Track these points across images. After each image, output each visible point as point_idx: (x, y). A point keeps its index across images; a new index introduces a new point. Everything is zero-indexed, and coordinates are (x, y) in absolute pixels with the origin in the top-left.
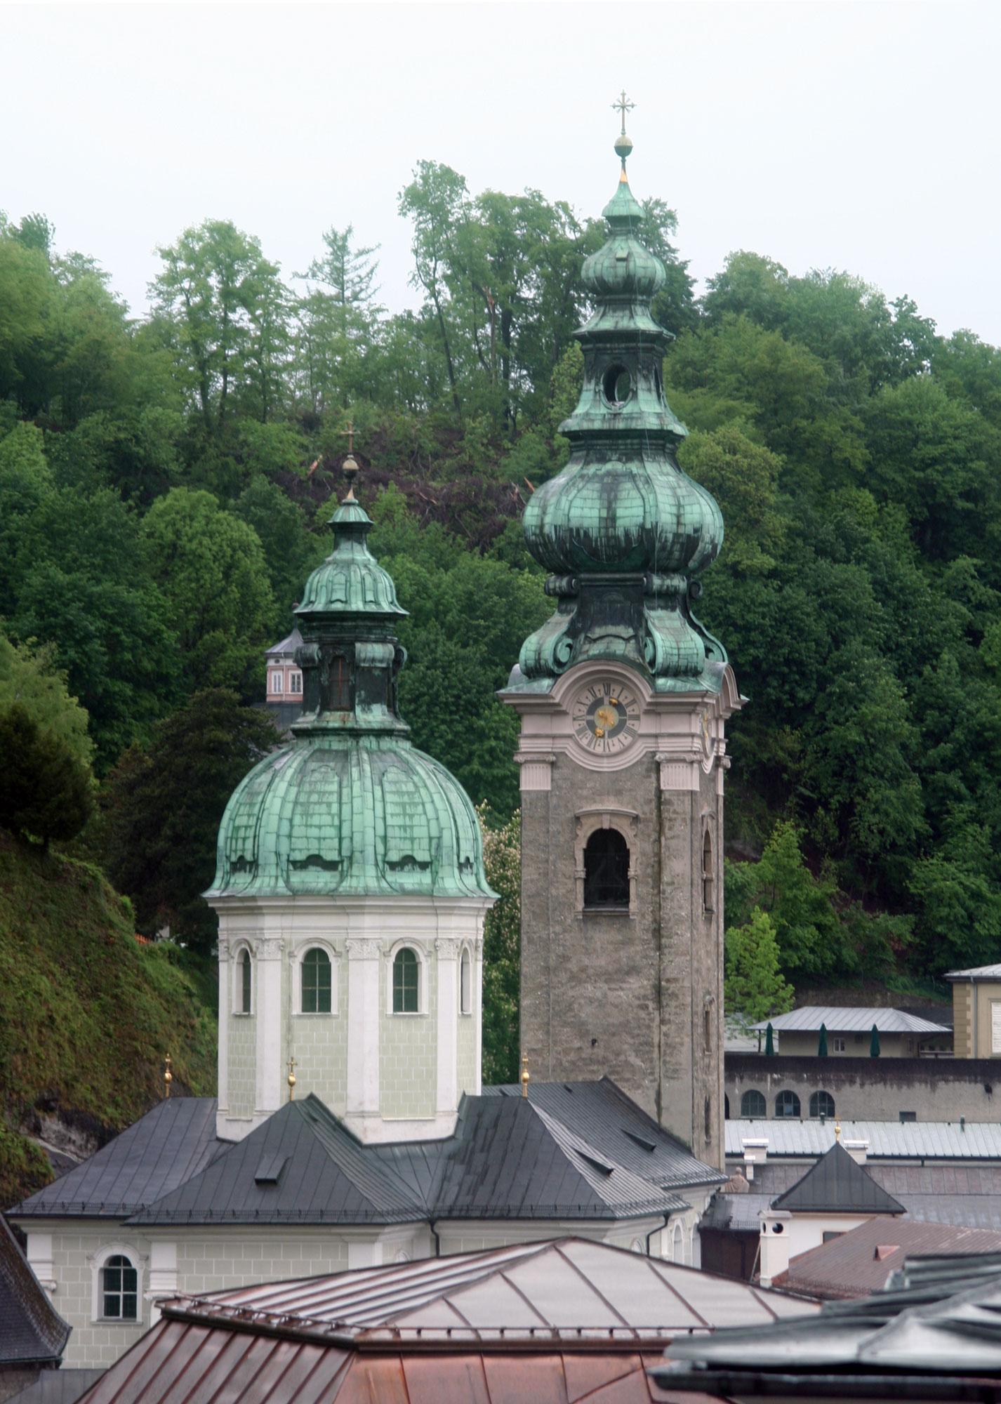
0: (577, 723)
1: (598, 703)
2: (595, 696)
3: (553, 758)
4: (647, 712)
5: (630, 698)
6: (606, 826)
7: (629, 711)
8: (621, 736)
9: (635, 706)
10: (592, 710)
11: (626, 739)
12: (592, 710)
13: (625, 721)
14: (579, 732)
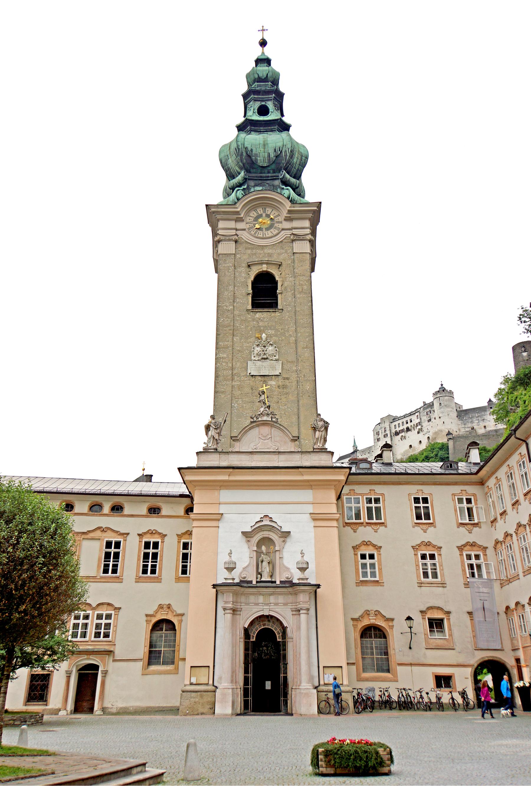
0: (248, 225)
1: (260, 216)
3: (236, 237)
4: (285, 220)
5: (277, 214)
6: (265, 269)
8: (272, 230)
9: (279, 217)
11: (274, 231)
13: (274, 224)
14: (249, 229)
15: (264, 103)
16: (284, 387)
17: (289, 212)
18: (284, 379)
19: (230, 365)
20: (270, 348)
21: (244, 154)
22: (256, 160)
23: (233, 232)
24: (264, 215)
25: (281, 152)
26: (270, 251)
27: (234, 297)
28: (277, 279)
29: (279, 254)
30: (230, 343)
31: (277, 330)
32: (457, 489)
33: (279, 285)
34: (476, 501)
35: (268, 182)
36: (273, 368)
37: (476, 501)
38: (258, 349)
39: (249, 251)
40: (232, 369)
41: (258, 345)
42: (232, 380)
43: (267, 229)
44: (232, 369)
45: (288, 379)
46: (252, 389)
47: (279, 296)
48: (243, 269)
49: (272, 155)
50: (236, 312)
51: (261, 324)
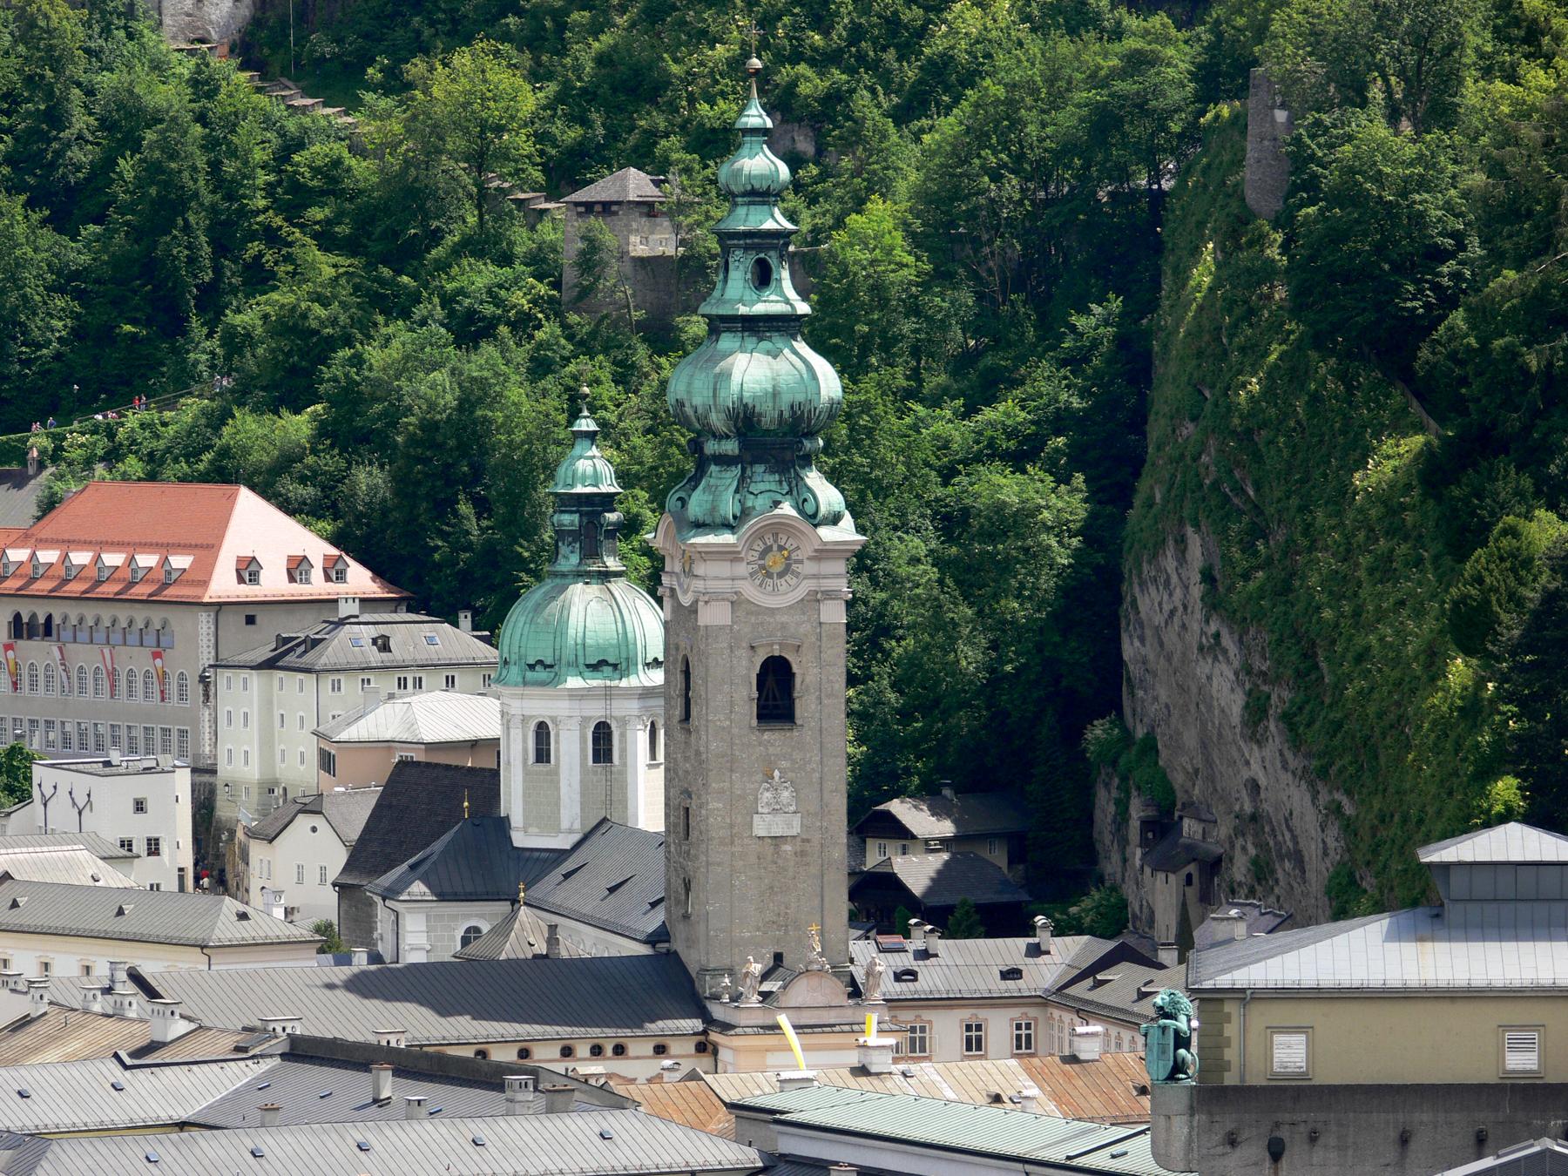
1: (768, 549)
2: (765, 544)
7: (794, 556)
8: (787, 577)
10: (763, 555)
12: (763, 555)
13: (790, 565)
14: (751, 575)
15: (762, 255)
16: (803, 853)
17: (816, 551)
18: (804, 841)
19: (728, 821)
20: (786, 794)
21: (742, 415)
22: (759, 421)
23: (726, 586)
24: (775, 548)
25: (803, 412)
26: (785, 619)
27: (732, 704)
28: (795, 669)
29: (798, 624)
30: (727, 785)
31: (794, 762)
32: (1015, 1013)
33: (798, 680)
34: (1036, 1026)
35: (773, 452)
36: (790, 825)
37: (1036, 1026)
38: (768, 795)
39: (753, 619)
40: (731, 826)
41: (768, 790)
42: (732, 843)
43: (781, 575)
44: (731, 826)
45: (808, 841)
46: (759, 858)
47: (797, 701)
48: (743, 653)
49: (786, 415)
50: (735, 731)
51: (771, 750)
